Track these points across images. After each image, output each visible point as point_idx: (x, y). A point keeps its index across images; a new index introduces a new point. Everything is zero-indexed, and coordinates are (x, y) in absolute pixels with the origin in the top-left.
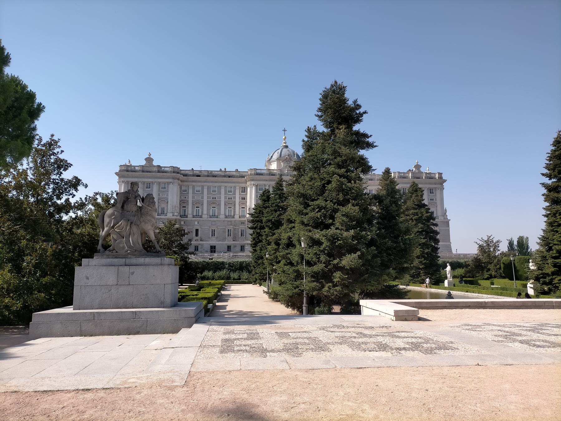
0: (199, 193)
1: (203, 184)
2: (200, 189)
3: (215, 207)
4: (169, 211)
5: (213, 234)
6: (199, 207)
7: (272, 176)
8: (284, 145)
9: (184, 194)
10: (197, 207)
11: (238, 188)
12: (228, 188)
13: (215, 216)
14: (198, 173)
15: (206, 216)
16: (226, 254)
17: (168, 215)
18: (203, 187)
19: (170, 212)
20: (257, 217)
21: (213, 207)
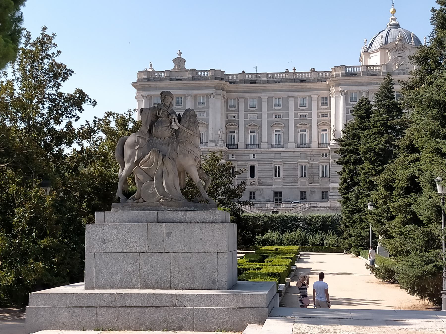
0: (254, 109)
1: (259, 94)
2: (255, 102)
3: (279, 131)
4: (210, 139)
5: (278, 174)
6: (254, 132)
7: (373, 77)
10: (251, 132)
11: (316, 98)
12: (299, 99)
13: (279, 144)
14: (252, 78)
15: (266, 145)
16: (299, 205)
17: (208, 145)
18: (260, 99)
19: (212, 141)
20: (350, 144)
21: (276, 131)
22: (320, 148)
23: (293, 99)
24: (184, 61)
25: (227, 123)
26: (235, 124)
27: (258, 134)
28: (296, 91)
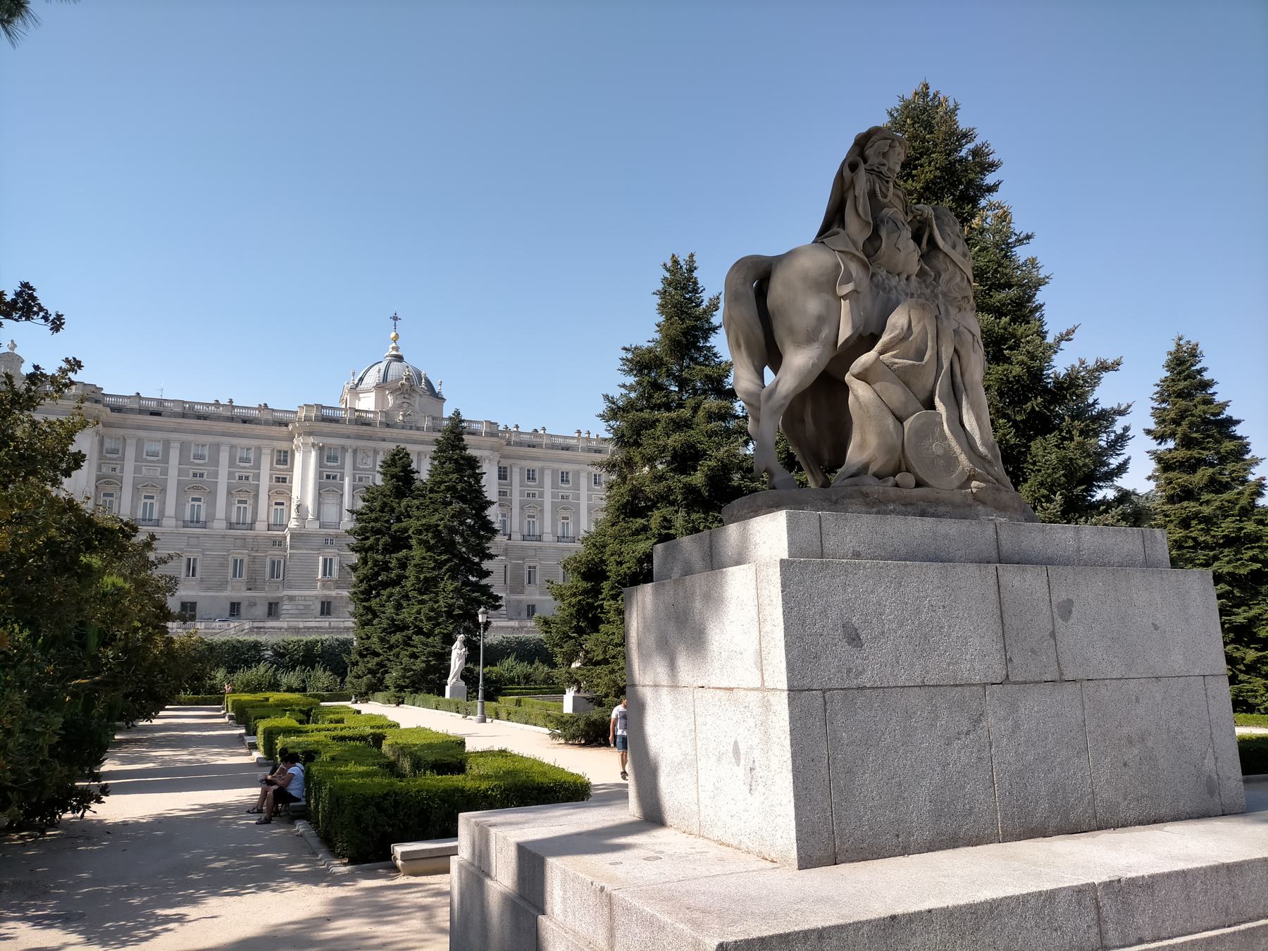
0: (155, 458)
2: (158, 447)
3: (199, 500)
6: (152, 497)
7: (364, 428)
8: (394, 353)
9: (110, 459)
10: (146, 497)
11: (269, 451)
12: (239, 449)
13: (198, 522)
14: (153, 405)
15: (173, 522)
18: (167, 444)
21: (194, 499)
22: (270, 532)
23: (228, 449)
24: (21, 360)
25: (98, 479)
26: (115, 481)
27: (158, 503)
28: (235, 436)
